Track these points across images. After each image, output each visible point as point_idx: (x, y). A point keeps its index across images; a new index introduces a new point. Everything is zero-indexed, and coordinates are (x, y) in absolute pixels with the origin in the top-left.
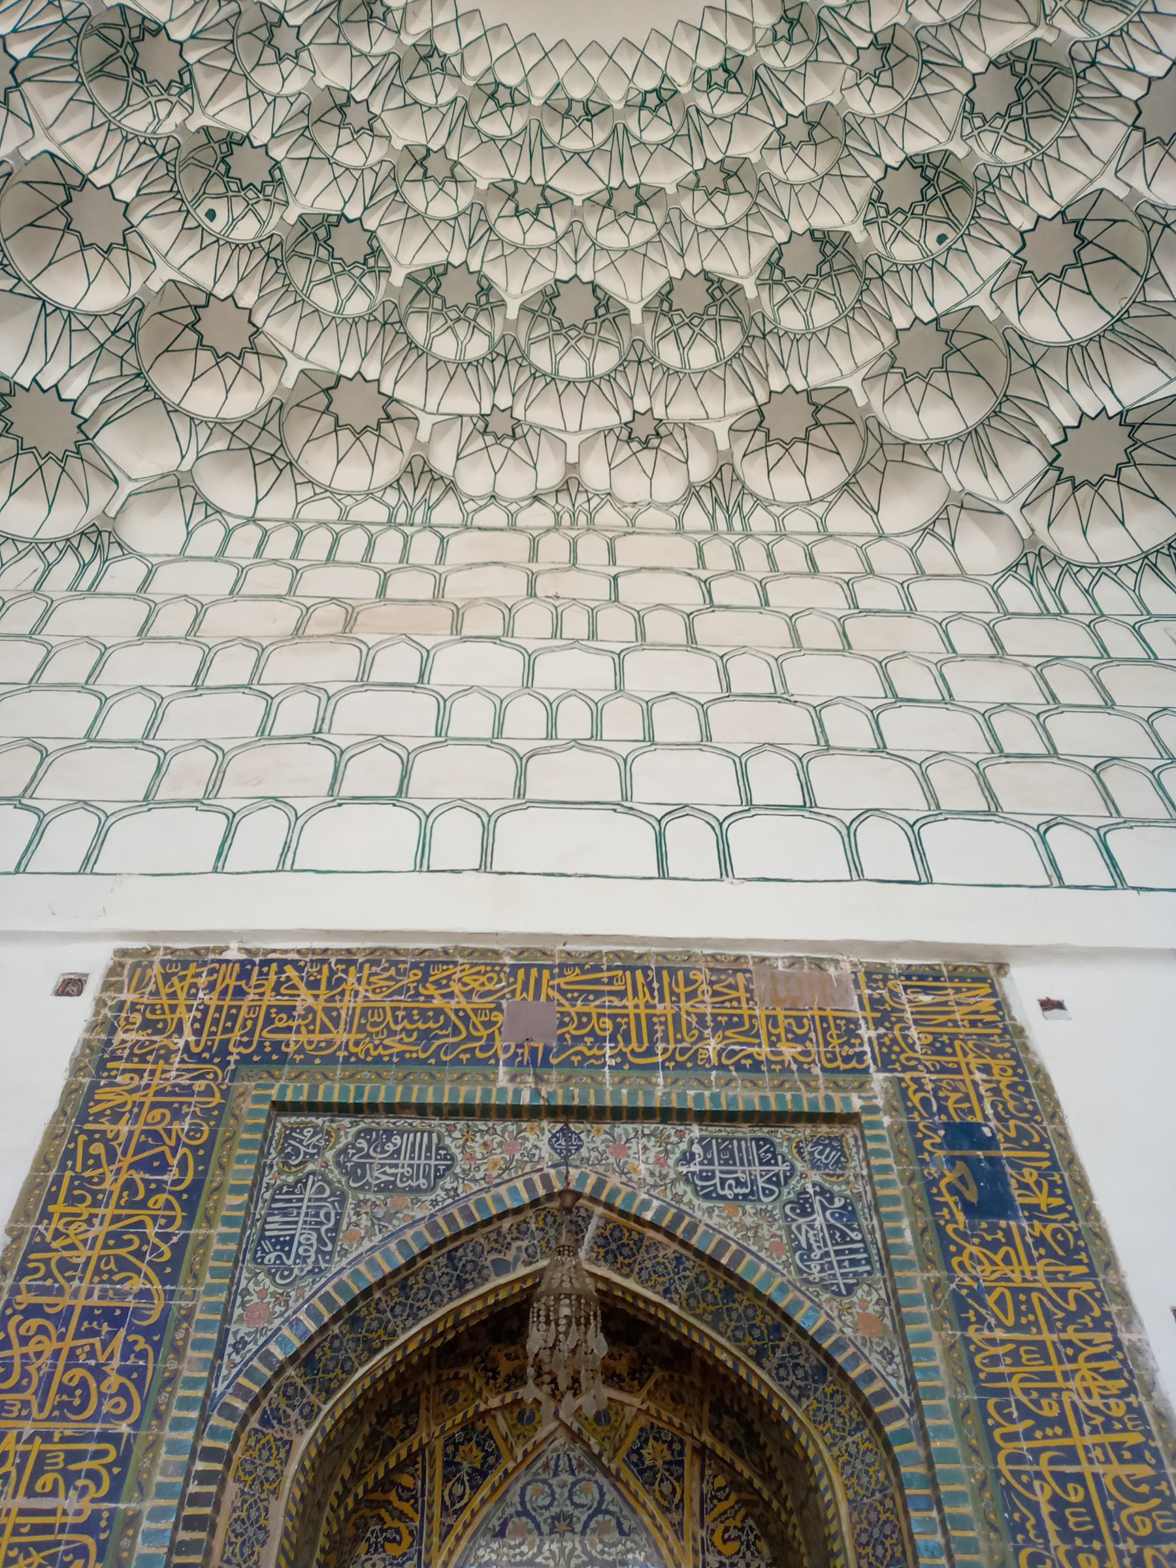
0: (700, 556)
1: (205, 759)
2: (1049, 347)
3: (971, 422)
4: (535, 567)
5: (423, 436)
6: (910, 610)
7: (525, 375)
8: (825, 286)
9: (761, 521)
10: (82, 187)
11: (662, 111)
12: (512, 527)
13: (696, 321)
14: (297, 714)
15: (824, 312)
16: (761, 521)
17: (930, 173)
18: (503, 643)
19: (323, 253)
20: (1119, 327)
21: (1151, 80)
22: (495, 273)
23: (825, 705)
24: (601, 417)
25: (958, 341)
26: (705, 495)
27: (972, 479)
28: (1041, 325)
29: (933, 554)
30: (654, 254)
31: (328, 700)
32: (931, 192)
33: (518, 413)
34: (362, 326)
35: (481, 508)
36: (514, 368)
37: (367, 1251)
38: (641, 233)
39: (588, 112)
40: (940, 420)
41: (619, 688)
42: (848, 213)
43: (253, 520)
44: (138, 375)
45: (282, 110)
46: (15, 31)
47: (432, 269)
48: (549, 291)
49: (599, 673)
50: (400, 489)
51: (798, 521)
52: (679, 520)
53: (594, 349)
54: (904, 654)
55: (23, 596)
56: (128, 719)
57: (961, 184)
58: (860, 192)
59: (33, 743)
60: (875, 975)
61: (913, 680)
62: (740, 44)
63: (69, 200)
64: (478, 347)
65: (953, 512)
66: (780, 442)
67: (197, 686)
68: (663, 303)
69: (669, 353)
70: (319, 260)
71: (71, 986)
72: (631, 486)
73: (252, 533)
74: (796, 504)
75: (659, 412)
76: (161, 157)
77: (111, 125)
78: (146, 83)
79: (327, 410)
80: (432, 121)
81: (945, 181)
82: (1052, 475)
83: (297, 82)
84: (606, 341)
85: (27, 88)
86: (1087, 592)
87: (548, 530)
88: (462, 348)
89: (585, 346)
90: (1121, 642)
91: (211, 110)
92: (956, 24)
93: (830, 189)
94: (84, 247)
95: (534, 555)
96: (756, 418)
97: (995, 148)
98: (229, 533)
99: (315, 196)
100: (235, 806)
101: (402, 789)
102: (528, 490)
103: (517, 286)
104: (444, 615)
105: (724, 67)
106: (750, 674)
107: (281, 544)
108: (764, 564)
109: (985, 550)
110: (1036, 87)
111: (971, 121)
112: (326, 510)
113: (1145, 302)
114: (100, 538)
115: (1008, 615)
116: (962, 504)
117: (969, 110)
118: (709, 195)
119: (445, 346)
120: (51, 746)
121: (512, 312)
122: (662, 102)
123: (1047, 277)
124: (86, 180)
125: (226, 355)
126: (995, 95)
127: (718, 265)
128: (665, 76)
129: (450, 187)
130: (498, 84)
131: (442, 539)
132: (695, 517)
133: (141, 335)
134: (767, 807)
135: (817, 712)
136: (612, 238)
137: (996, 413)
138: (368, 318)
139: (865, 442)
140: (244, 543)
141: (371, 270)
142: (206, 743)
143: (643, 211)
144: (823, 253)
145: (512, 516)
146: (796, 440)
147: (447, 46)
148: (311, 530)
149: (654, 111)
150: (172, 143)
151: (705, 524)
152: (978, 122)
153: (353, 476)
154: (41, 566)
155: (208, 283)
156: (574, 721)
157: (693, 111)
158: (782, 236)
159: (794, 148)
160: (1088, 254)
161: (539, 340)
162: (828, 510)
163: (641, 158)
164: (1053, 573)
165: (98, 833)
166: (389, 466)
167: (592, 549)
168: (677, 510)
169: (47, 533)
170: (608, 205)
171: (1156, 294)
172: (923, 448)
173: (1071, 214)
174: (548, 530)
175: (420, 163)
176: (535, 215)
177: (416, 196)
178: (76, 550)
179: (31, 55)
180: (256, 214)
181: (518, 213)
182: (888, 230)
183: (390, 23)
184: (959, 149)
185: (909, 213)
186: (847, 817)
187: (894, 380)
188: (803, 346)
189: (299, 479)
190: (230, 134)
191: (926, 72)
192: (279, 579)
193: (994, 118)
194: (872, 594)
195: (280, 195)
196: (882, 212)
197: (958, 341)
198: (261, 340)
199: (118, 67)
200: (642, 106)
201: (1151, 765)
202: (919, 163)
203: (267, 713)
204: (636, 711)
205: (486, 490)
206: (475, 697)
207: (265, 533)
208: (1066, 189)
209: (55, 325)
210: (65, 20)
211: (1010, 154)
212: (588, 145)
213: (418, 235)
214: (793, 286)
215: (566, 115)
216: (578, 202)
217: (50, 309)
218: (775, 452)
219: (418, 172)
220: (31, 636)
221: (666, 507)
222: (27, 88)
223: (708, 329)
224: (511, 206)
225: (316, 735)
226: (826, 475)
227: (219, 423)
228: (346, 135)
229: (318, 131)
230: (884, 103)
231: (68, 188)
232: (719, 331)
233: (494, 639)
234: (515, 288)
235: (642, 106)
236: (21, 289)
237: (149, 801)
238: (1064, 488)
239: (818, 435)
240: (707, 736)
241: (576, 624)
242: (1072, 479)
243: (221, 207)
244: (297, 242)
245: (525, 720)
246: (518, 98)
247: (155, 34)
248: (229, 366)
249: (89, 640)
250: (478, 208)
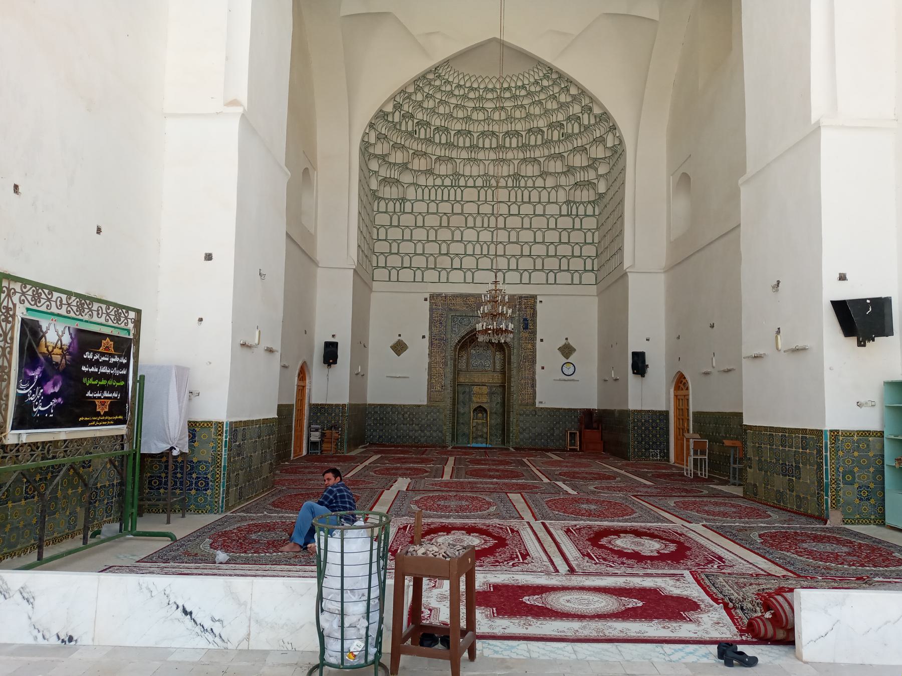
9: (522, 184)
24: (493, 156)
37: (463, 332)
60: (521, 297)
62: (526, 82)
68: (507, 133)
71: (426, 300)
109: (562, 196)
117: (569, 119)
132: (510, 184)
136: (496, 116)
147: (462, 83)
213: (455, 121)
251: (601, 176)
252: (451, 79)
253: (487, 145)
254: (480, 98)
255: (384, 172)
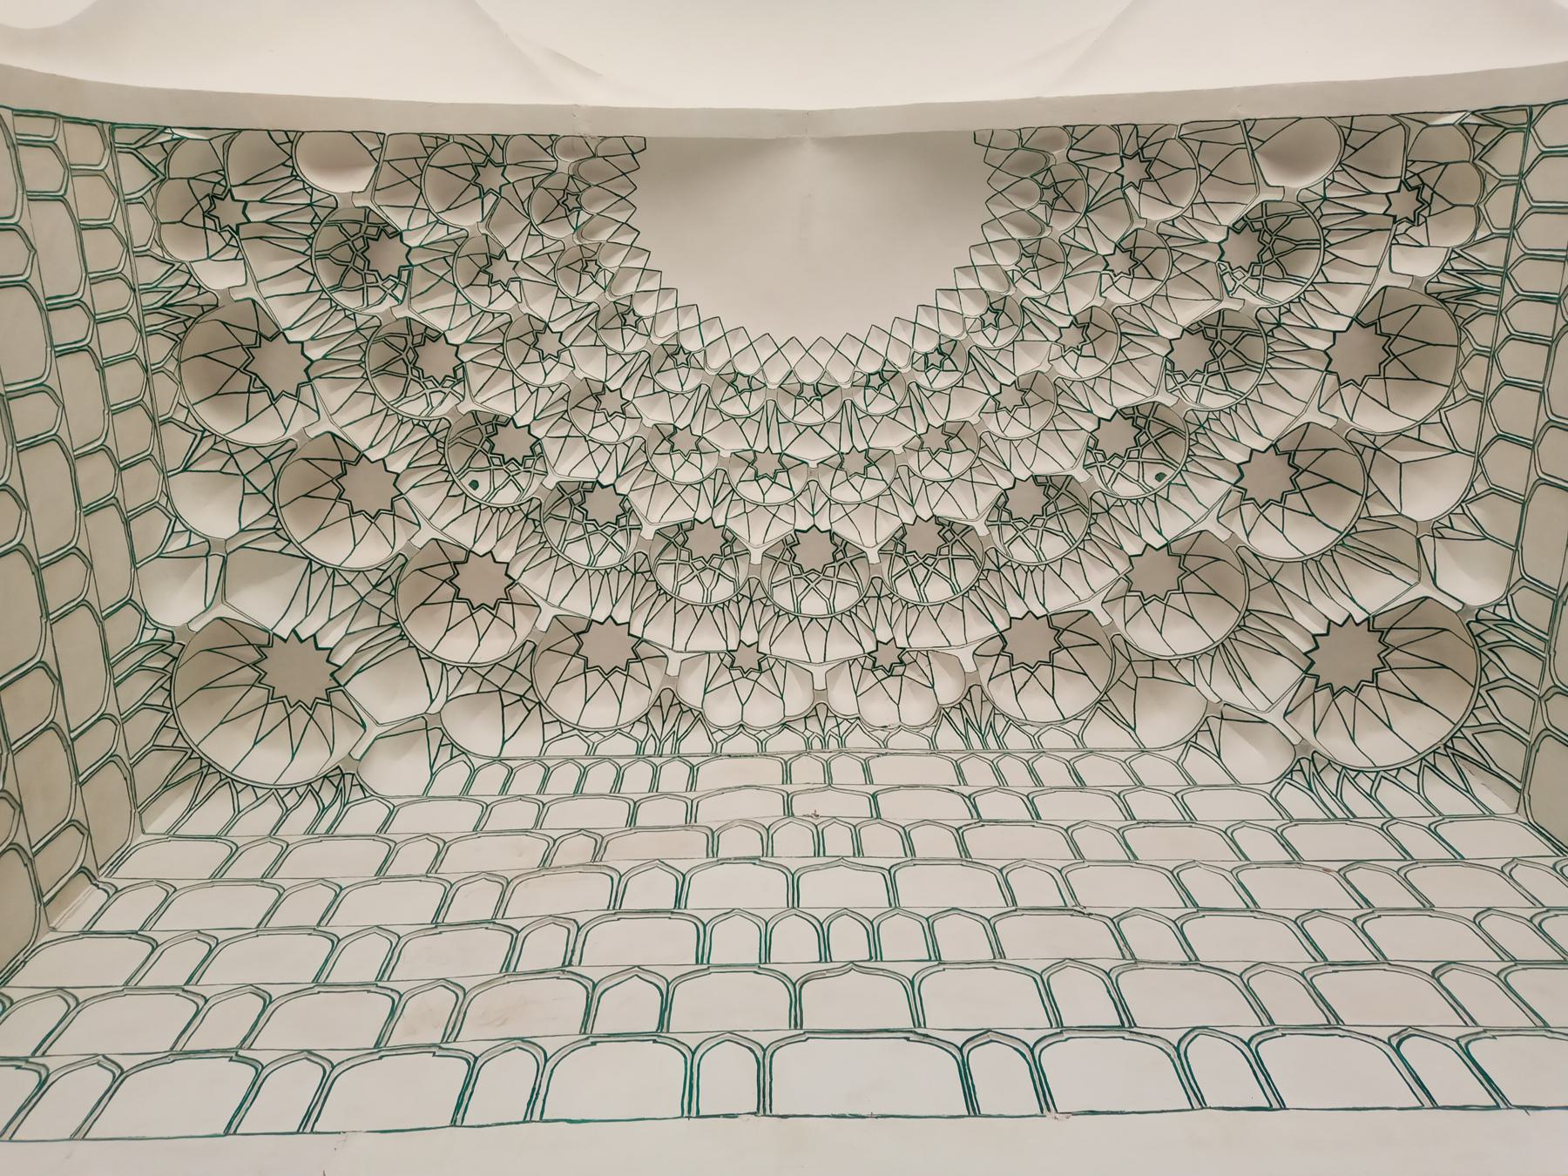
0: (959, 772)
1: (443, 1000)
2: (1283, 562)
3: (1218, 635)
4: (789, 788)
5: (673, 670)
6: (1190, 820)
7: (770, 613)
8: (1051, 524)
9: (1015, 739)
10: (358, 461)
11: (885, 390)
12: (762, 753)
13: (930, 561)
14: (545, 948)
15: (1053, 547)
16: (1015, 739)
17: (1141, 422)
18: (763, 864)
19: (578, 515)
20: (1348, 541)
21: (1335, 333)
22: (739, 527)
23: (1122, 916)
25: (1191, 563)
26: (956, 716)
27: (1225, 690)
28: (1268, 543)
29: (1199, 765)
30: (885, 504)
31: (577, 931)
32: (1143, 439)
33: (764, 648)
34: (613, 575)
35: (729, 737)
36: (758, 607)
38: (871, 489)
39: (817, 392)
40: (1184, 638)
41: (894, 904)
42: (1067, 461)
43: (499, 760)
44: (394, 625)
45: (544, 397)
46: (312, 339)
47: (680, 525)
48: (790, 540)
49: (868, 892)
50: (648, 723)
51: (1052, 739)
52: (932, 741)
53: (833, 588)
54: (1194, 863)
55: (259, 841)
56: (361, 961)
57: (1171, 430)
58: (1077, 443)
59: (256, 991)
61: (1209, 888)
62: (952, 331)
63: (344, 473)
64: (723, 591)
65: (1214, 724)
66: (1024, 666)
67: (437, 924)
69: (906, 588)
70: (574, 521)
72: (878, 710)
73: (499, 772)
74: (1048, 723)
75: (901, 642)
76: (432, 436)
77: (388, 410)
78: (422, 378)
79: (577, 654)
80: (679, 404)
81: (1156, 429)
82: (1309, 682)
83: (558, 375)
84: (844, 582)
85: (317, 382)
86: (1369, 796)
87: (800, 755)
88: (707, 592)
89: (825, 588)
90: (1421, 844)
91: (479, 399)
92: (1148, 303)
93: (1046, 441)
94: (353, 513)
95: (787, 776)
96: (998, 643)
97: (1199, 397)
98: (474, 772)
99: (570, 466)
100: (477, 1049)
101: (663, 1022)
102: (776, 718)
103: (758, 536)
104: (699, 840)
105: (939, 350)
106: (1034, 888)
107: (528, 780)
108: (1027, 779)
109: (1255, 760)
110: (1229, 348)
111: (1173, 377)
112: (575, 746)
113: (1369, 518)
114: (342, 781)
115: (1294, 822)
116: (1220, 715)
118: (933, 455)
119: (692, 592)
120: (275, 992)
121: (756, 558)
122: (885, 381)
123: (1269, 503)
124: (361, 455)
125: (481, 606)
126: (1193, 354)
127: (947, 510)
128: (886, 361)
129: (695, 458)
130: (737, 374)
131: (692, 767)
132: (948, 738)
133: (401, 588)
134: (1081, 1028)
135: (1115, 924)
136: (845, 494)
137: (1241, 627)
138: (621, 568)
139: (1113, 660)
140: (490, 780)
141: (623, 528)
142: (446, 983)
143: (872, 471)
144: (1047, 496)
145: (761, 744)
146: (1040, 663)
147: (692, 344)
148: (557, 766)
149: (878, 389)
150: (444, 424)
151: (959, 744)
152: (1180, 378)
153: (601, 713)
154: (279, 812)
155: (468, 544)
156: (849, 942)
157: (913, 387)
158: (1006, 483)
159: (1009, 412)
160: (1304, 480)
161: (781, 583)
162: (1084, 727)
163: (868, 426)
164: (1331, 779)
165: (322, 1085)
166: (637, 702)
167: (847, 770)
168: (928, 732)
169: (287, 780)
170: (840, 467)
171: (1378, 509)
172: (1172, 663)
173: (1282, 446)
174: (800, 755)
175: (668, 438)
176: (773, 480)
177: (664, 466)
178: (316, 795)
179: (324, 357)
180: (516, 484)
181: (757, 478)
182: (1107, 473)
183: (642, 328)
184: (1169, 400)
185: (1126, 457)
186: (1174, 1037)
187: (1133, 603)
188: (1038, 575)
189: (547, 718)
190: (496, 417)
191: (1125, 341)
192: (524, 814)
193: (1194, 374)
194: (1143, 805)
195: (540, 466)
196: (1100, 458)
197: (1191, 563)
198: (516, 591)
199: (400, 367)
200: (867, 386)
201: (1496, 967)
202: (1130, 415)
203: (512, 947)
204: (915, 928)
205: (736, 719)
206: (737, 920)
207: (511, 771)
208: (1273, 427)
209: (319, 580)
210: (358, 330)
211: (1212, 401)
212: (819, 419)
213: (665, 497)
214: (1021, 525)
215: (799, 396)
216: (813, 465)
217: (315, 566)
218: (1020, 675)
219: (666, 446)
220: (263, 880)
221: (916, 730)
222: (317, 382)
223: (943, 567)
224: (751, 471)
225: (566, 968)
226: (1075, 695)
227: (471, 667)
228: (600, 418)
229: (574, 414)
230: (1088, 369)
231: (344, 463)
232: (952, 569)
233: (752, 860)
234: (757, 538)
235: (867, 386)
236: (291, 550)
237: (380, 1048)
238: (1324, 695)
239: (1062, 657)
240: (999, 952)
241: (837, 840)
242: (1329, 686)
243: (484, 479)
244: (554, 506)
245: (795, 945)
246: (755, 384)
247: (435, 340)
248: (483, 617)
249: (323, 881)
250: (722, 472)
251: (1437, 530)
252: (645, 309)
253: (813, 605)
254: (770, 418)
255: (262, 604)
